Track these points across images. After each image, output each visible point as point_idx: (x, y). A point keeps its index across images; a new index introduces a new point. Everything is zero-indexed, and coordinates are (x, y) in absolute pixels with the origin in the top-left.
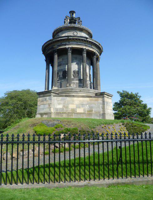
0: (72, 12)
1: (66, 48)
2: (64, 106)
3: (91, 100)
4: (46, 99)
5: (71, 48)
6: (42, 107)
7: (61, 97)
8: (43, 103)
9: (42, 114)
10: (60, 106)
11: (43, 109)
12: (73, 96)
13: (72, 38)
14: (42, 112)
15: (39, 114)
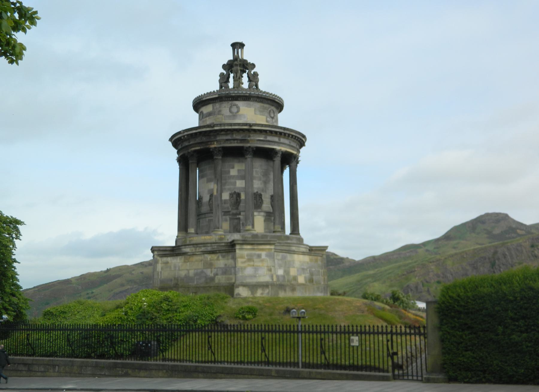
0: (237, 46)
1: (273, 149)
2: (285, 271)
3: (311, 260)
4: (259, 256)
5: (282, 152)
6: (249, 271)
7: (281, 254)
8: (252, 263)
9: (253, 287)
10: (280, 272)
11: (251, 276)
12: (294, 252)
13: (288, 132)
14: (254, 281)
15: (244, 285)
